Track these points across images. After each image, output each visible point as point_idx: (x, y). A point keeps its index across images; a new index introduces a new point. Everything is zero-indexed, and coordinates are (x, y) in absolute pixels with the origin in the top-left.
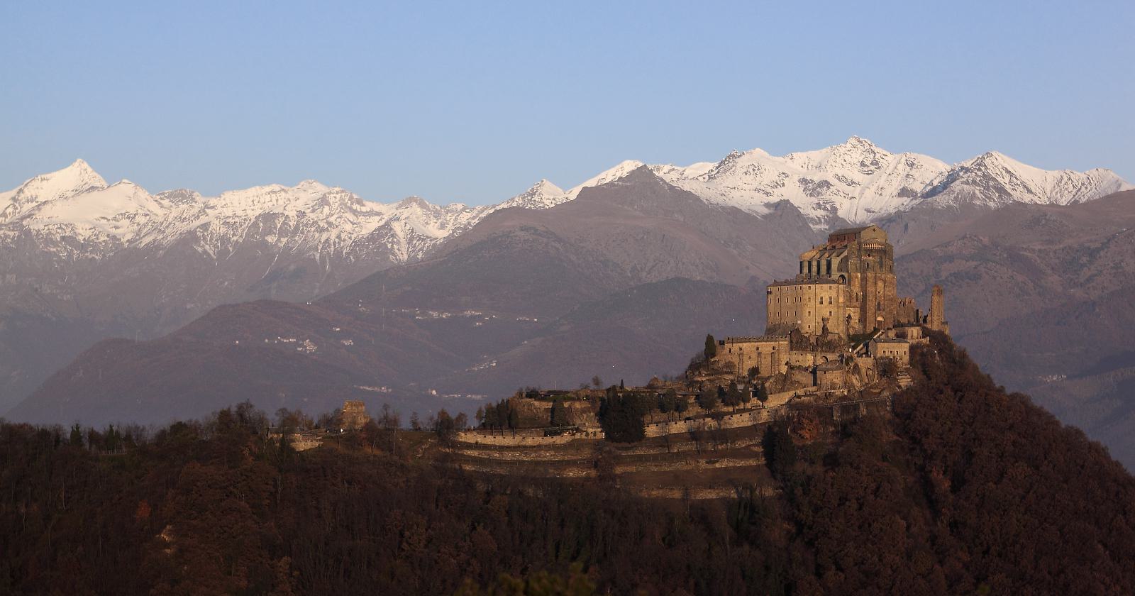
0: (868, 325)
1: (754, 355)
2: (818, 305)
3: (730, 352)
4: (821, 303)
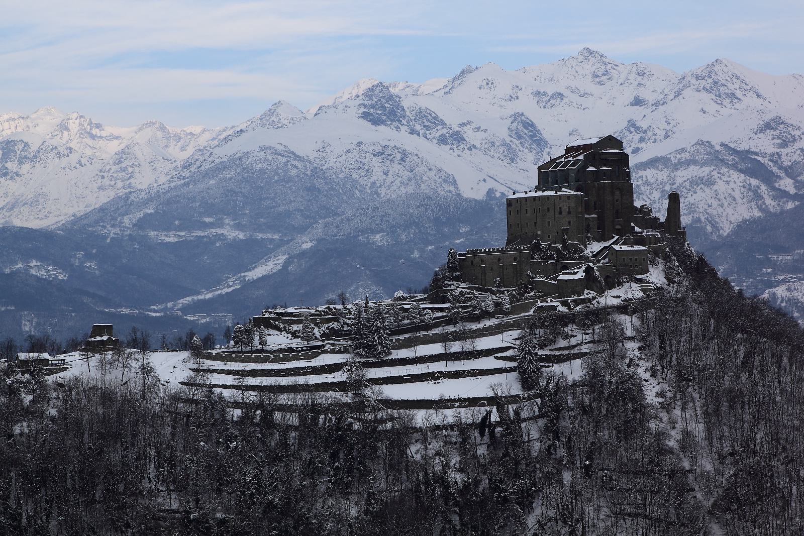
0: (606, 233)
2: (557, 216)
3: (472, 264)
4: (560, 213)
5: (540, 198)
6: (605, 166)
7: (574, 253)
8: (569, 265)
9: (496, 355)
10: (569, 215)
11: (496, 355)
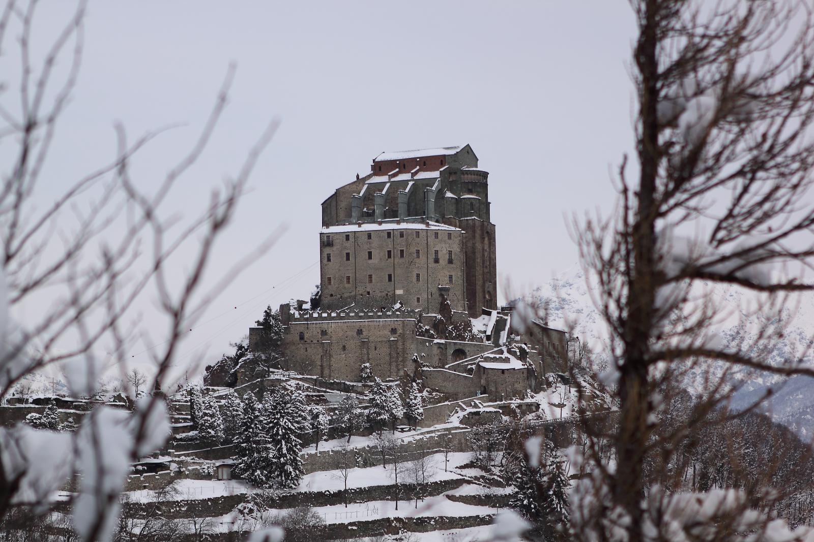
1: (352, 344)
2: (432, 265)
4: (437, 261)
5: (402, 233)
6: (470, 192)
7: (465, 331)
8: (467, 349)
9: (450, 493)
10: (452, 266)
11: (450, 493)
